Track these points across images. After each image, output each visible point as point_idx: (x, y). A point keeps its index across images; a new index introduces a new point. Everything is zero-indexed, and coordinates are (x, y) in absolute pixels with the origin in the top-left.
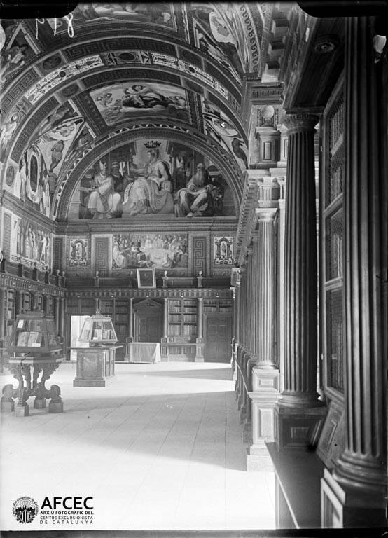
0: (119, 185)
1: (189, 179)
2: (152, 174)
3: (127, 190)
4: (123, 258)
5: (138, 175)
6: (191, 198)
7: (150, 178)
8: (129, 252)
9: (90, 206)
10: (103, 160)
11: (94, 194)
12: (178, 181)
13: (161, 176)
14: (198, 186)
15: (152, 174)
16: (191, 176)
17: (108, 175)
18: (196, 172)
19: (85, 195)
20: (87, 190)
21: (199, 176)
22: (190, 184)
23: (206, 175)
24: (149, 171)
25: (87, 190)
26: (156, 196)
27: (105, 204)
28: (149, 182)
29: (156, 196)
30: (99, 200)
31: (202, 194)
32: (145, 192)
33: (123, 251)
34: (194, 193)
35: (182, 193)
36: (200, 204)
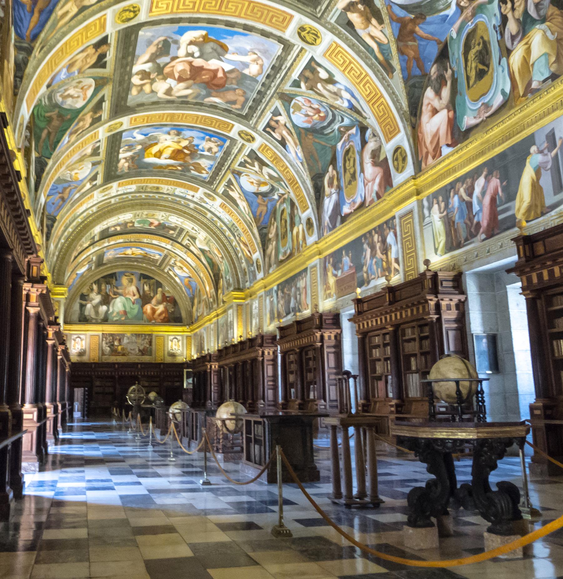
0: (106, 300)
1: (152, 298)
2: (129, 293)
3: (111, 304)
4: (108, 349)
5: (120, 295)
6: (154, 311)
7: (128, 296)
8: (113, 345)
9: (87, 313)
10: (95, 282)
11: (89, 306)
12: (145, 299)
13: (134, 295)
14: (159, 303)
15: (129, 293)
16: (154, 296)
17: (99, 292)
18: (157, 293)
19: (82, 306)
20: (84, 302)
21: (159, 296)
22: (154, 301)
23: (163, 295)
24: (127, 292)
25: (84, 302)
26: (131, 308)
27: (97, 313)
28: (126, 299)
29: (131, 308)
30: (93, 310)
31: (161, 308)
32: (124, 306)
33: (109, 345)
34: (156, 308)
35: (148, 308)
36: (160, 314)
